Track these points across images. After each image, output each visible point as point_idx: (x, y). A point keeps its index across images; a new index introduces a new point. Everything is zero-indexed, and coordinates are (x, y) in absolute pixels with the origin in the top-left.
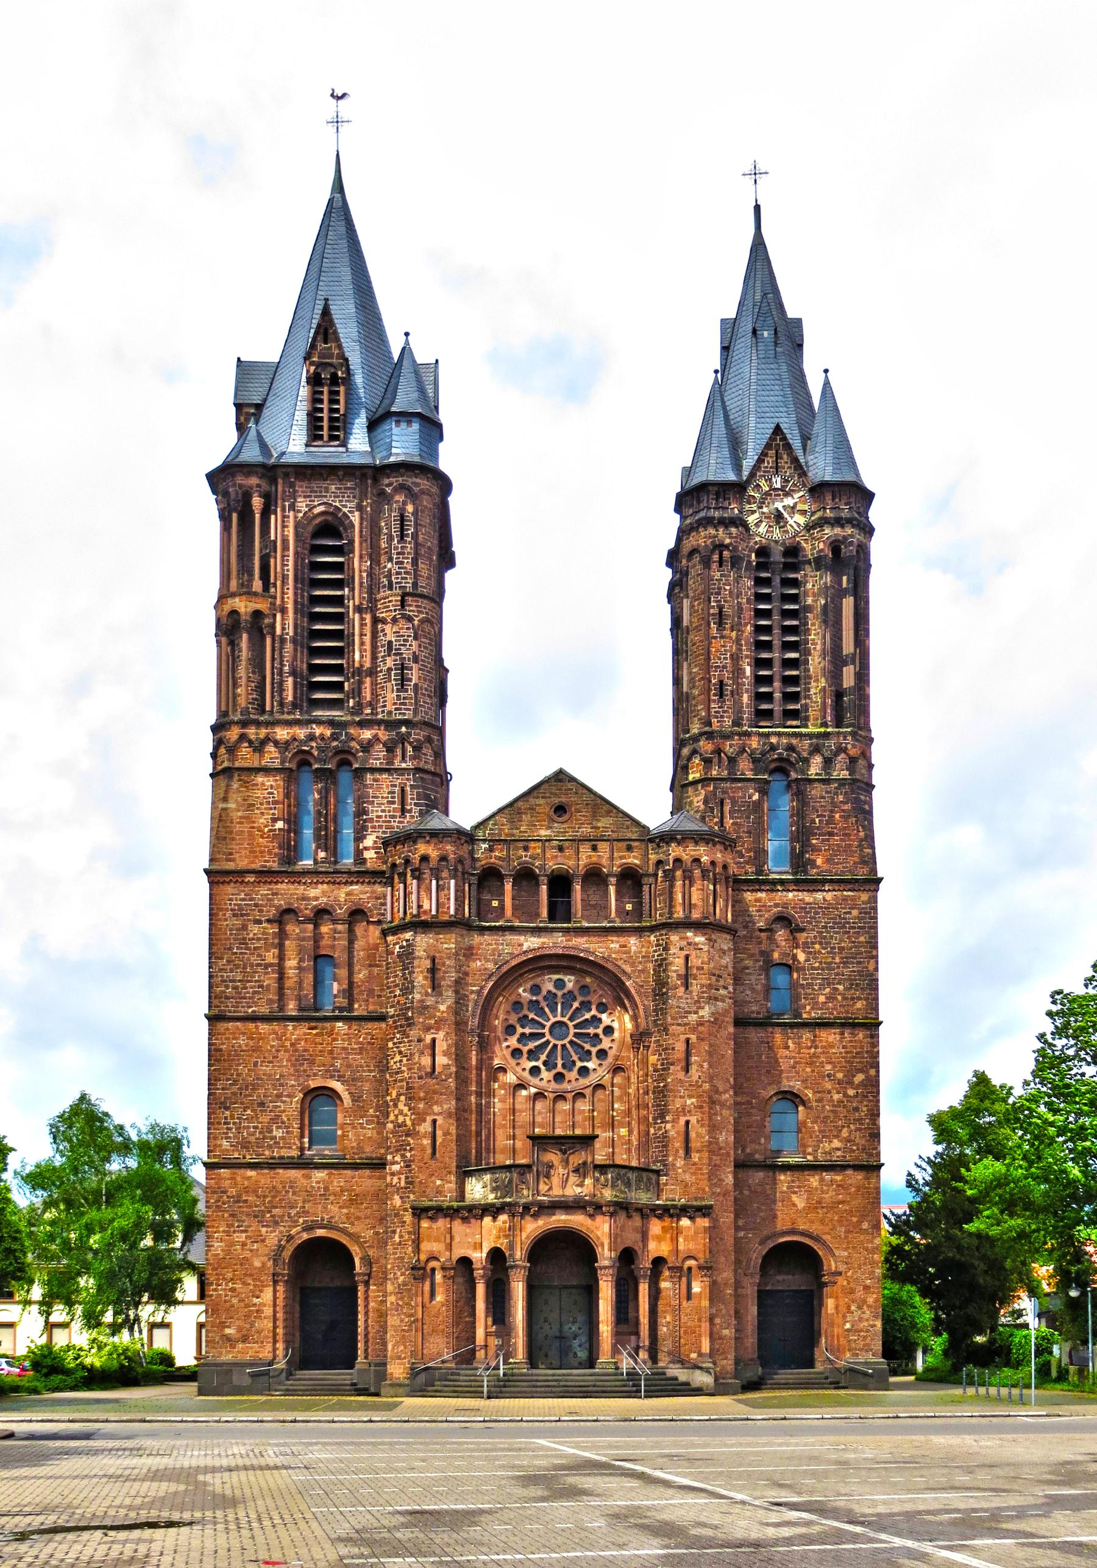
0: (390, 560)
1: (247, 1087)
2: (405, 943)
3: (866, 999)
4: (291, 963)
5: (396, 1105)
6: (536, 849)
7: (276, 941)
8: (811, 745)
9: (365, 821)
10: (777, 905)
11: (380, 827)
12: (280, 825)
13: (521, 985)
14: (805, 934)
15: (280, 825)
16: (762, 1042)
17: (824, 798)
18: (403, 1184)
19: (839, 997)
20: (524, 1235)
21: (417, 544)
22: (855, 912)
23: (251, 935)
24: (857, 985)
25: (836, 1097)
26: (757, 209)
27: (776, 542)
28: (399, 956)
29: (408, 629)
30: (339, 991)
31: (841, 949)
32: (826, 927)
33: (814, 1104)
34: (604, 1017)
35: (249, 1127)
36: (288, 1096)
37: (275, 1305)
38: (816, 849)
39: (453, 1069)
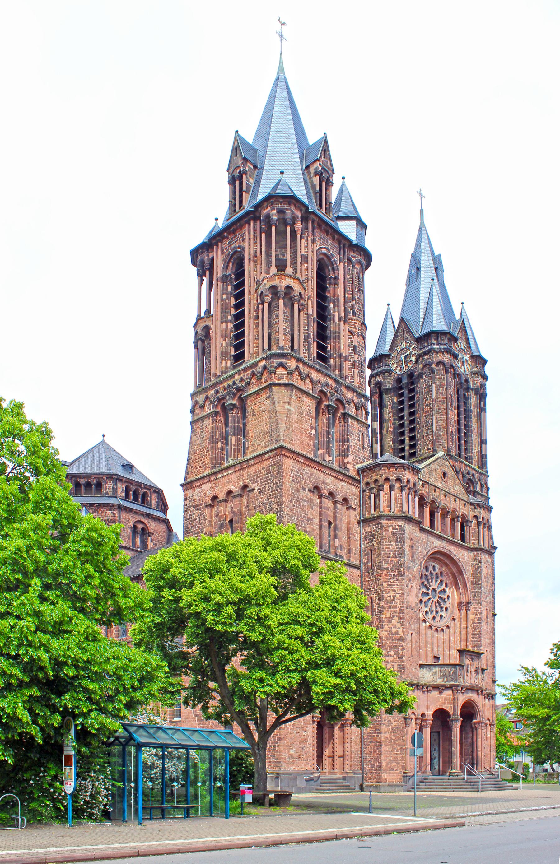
2: (397, 527)
9: (348, 446)
26: (422, 211)
28: (392, 534)
34: (447, 590)
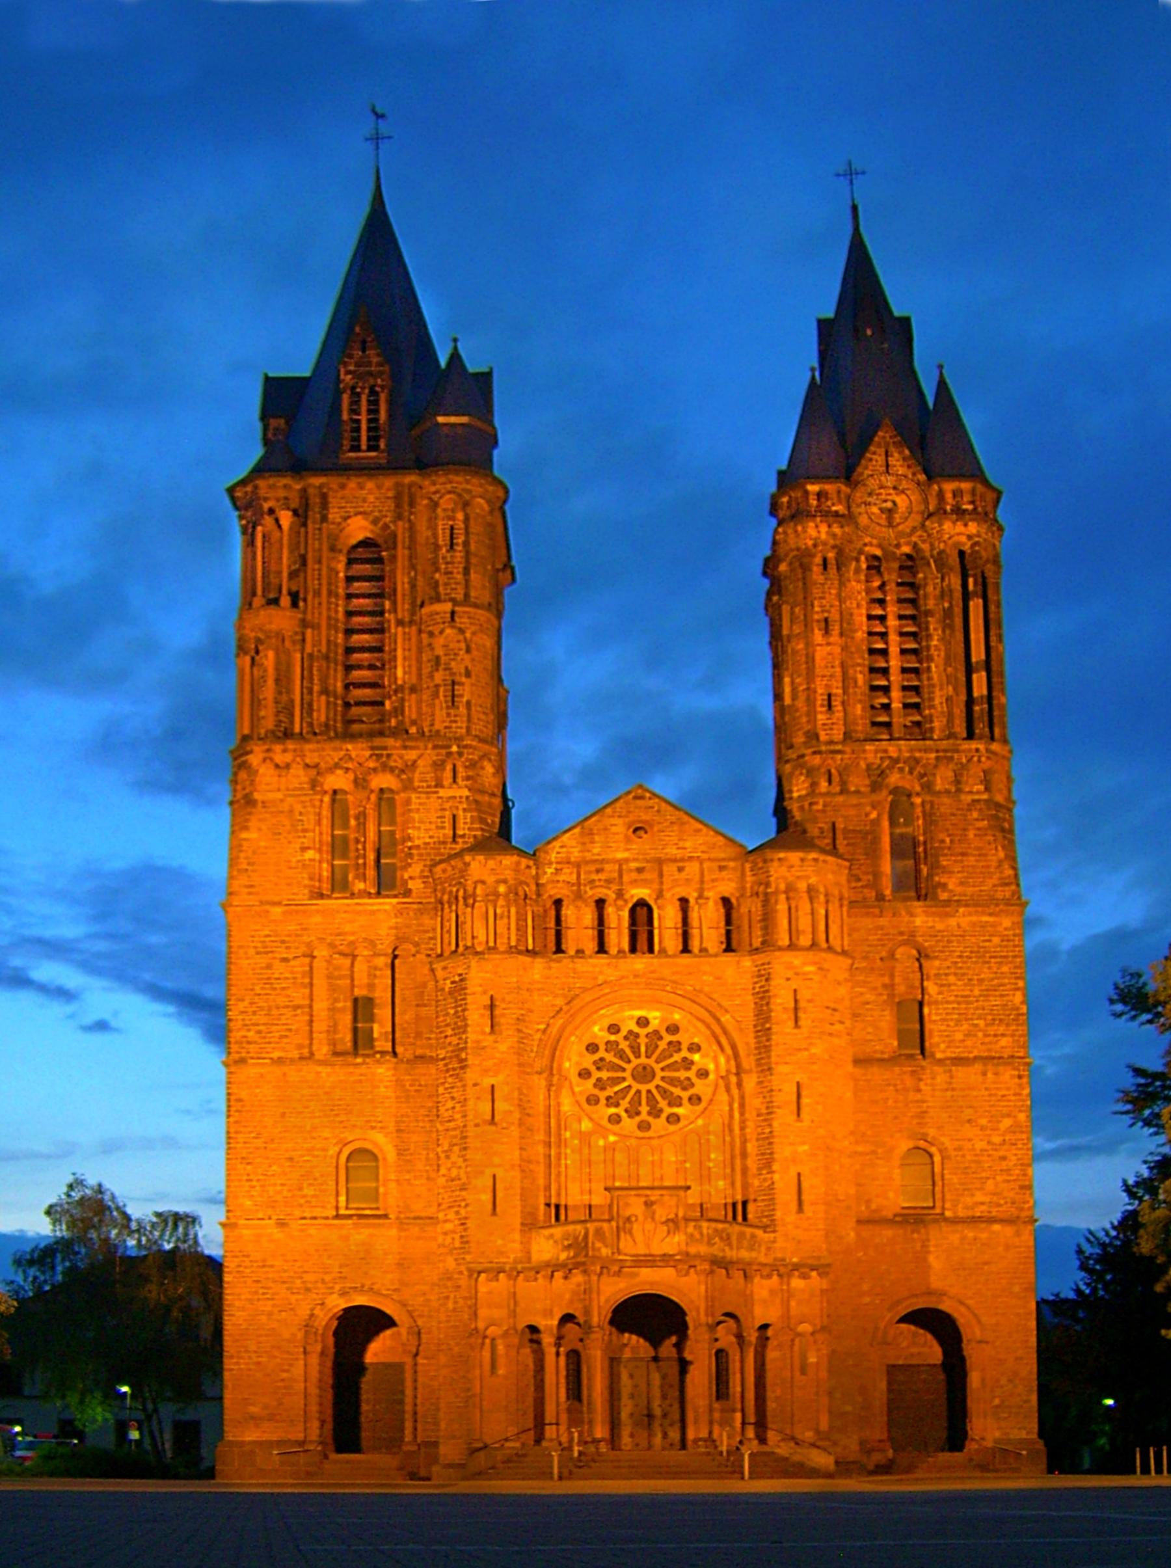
0: (437, 570)
3: (1013, 1036)
4: (320, 1006)
5: (448, 1157)
8: (937, 758)
10: (901, 934)
11: (429, 854)
13: (595, 1023)
14: (937, 963)
16: (889, 1085)
17: (954, 815)
18: (457, 1244)
19: (980, 1034)
20: (602, 1299)
21: (468, 553)
22: (996, 940)
24: (1001, 1020)
25: (980, 1145)
29: (459, 641)
31: (981, 981)
32: (960, 957)
33: (953, 1153)
35: (275, 1185)
38: (945, 871)
39: (517, 1115)
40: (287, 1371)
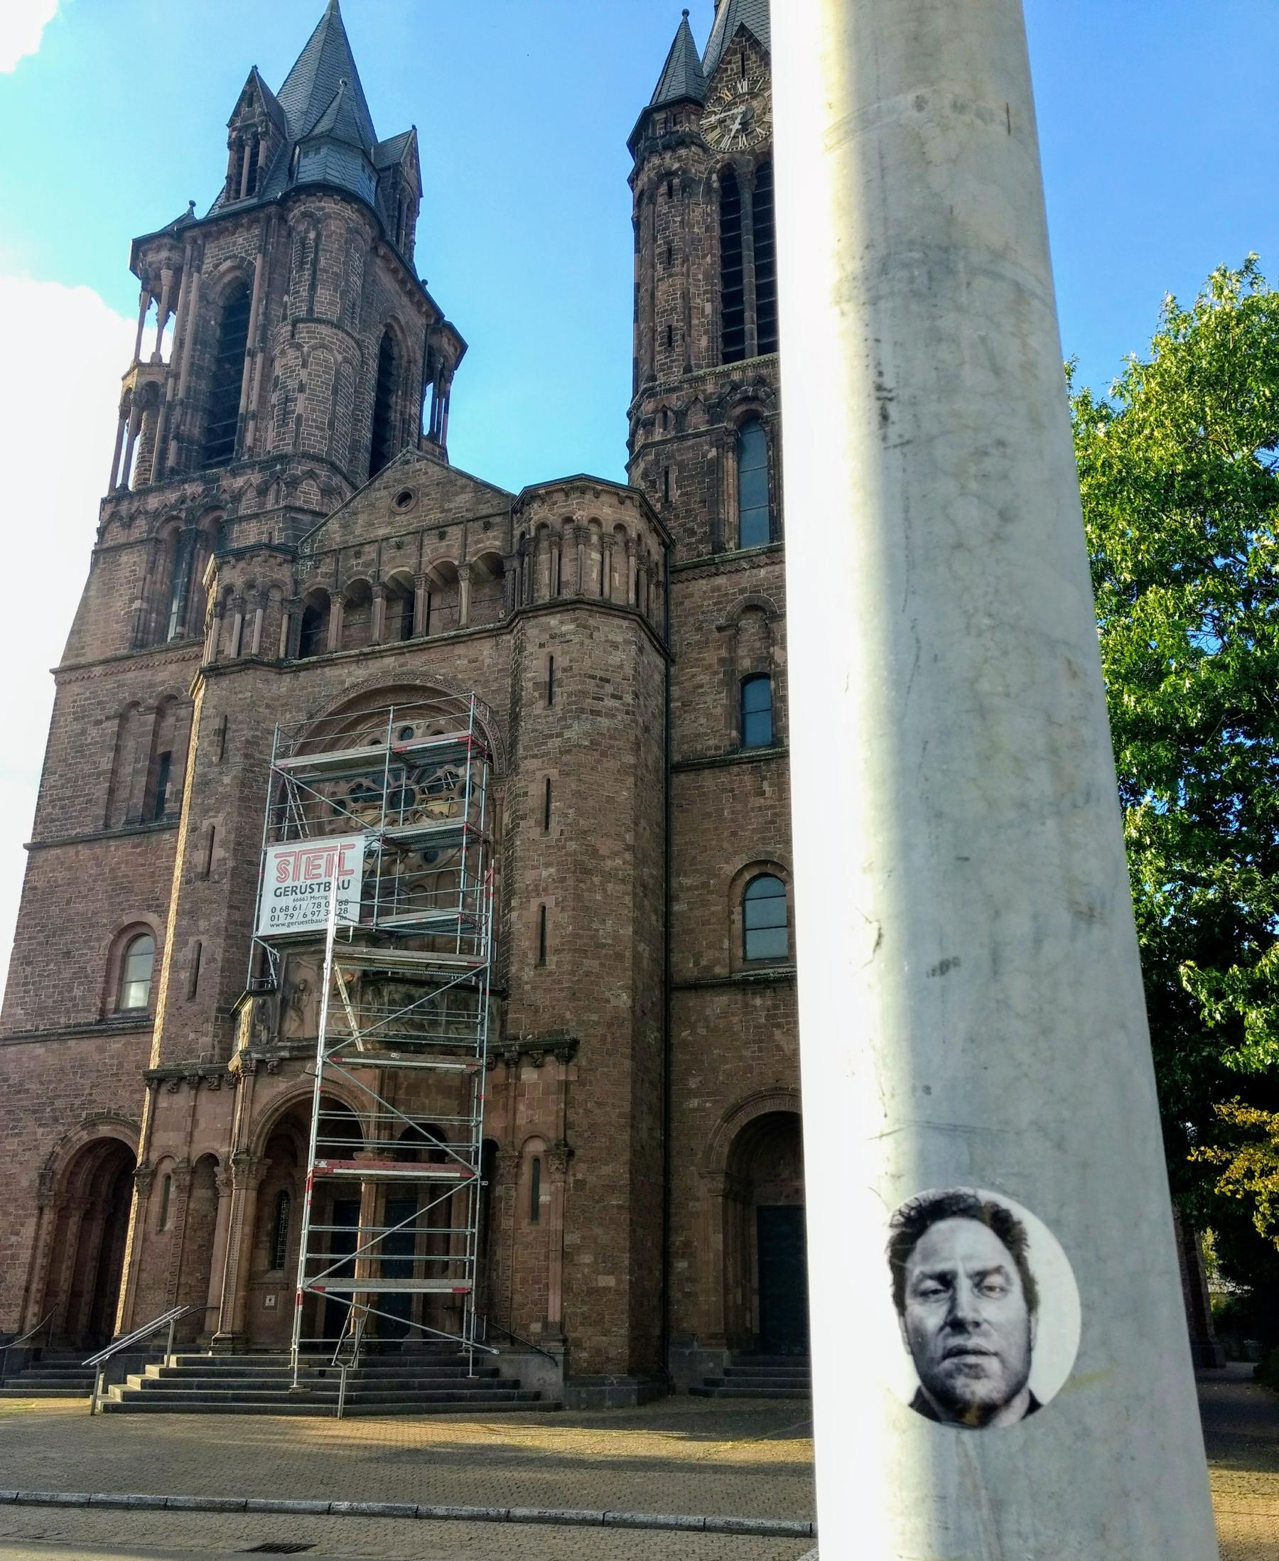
1: (54, 933)
6: (370, 552)
7: (114, 742)
12: (137, 604)
15: (137, 604)
23: (89, 740)
27: (743, 152)
30: (171, 794)
36: (99, 939)
37: (35, 1248)
40: (17, 1234)
